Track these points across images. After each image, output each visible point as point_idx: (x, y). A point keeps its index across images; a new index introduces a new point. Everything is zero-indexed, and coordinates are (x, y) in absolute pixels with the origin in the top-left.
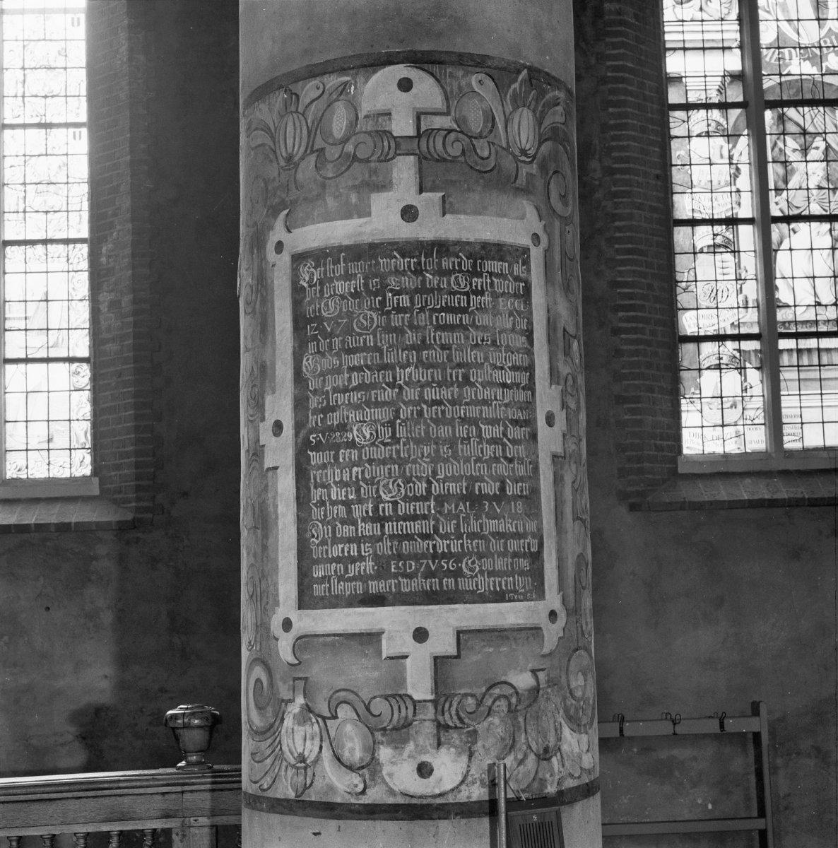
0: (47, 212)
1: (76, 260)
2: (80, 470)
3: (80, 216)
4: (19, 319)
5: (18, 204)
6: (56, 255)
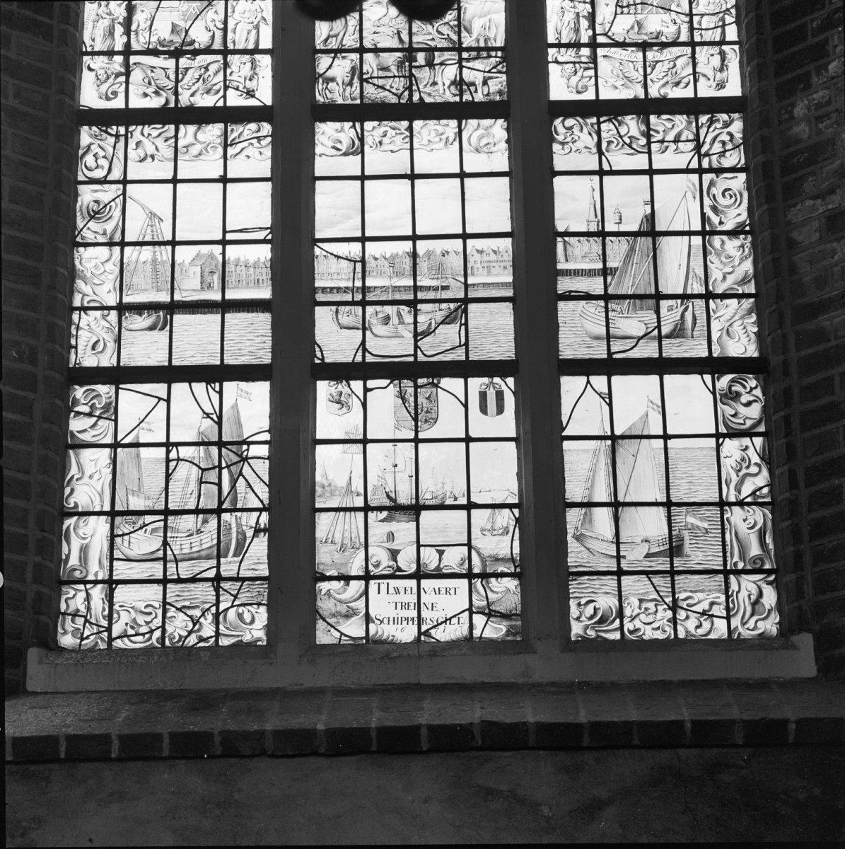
0: (644, 46)
1: (717, 148)
2: (751, 624)
4: (590, 273)
6: (671, 137)
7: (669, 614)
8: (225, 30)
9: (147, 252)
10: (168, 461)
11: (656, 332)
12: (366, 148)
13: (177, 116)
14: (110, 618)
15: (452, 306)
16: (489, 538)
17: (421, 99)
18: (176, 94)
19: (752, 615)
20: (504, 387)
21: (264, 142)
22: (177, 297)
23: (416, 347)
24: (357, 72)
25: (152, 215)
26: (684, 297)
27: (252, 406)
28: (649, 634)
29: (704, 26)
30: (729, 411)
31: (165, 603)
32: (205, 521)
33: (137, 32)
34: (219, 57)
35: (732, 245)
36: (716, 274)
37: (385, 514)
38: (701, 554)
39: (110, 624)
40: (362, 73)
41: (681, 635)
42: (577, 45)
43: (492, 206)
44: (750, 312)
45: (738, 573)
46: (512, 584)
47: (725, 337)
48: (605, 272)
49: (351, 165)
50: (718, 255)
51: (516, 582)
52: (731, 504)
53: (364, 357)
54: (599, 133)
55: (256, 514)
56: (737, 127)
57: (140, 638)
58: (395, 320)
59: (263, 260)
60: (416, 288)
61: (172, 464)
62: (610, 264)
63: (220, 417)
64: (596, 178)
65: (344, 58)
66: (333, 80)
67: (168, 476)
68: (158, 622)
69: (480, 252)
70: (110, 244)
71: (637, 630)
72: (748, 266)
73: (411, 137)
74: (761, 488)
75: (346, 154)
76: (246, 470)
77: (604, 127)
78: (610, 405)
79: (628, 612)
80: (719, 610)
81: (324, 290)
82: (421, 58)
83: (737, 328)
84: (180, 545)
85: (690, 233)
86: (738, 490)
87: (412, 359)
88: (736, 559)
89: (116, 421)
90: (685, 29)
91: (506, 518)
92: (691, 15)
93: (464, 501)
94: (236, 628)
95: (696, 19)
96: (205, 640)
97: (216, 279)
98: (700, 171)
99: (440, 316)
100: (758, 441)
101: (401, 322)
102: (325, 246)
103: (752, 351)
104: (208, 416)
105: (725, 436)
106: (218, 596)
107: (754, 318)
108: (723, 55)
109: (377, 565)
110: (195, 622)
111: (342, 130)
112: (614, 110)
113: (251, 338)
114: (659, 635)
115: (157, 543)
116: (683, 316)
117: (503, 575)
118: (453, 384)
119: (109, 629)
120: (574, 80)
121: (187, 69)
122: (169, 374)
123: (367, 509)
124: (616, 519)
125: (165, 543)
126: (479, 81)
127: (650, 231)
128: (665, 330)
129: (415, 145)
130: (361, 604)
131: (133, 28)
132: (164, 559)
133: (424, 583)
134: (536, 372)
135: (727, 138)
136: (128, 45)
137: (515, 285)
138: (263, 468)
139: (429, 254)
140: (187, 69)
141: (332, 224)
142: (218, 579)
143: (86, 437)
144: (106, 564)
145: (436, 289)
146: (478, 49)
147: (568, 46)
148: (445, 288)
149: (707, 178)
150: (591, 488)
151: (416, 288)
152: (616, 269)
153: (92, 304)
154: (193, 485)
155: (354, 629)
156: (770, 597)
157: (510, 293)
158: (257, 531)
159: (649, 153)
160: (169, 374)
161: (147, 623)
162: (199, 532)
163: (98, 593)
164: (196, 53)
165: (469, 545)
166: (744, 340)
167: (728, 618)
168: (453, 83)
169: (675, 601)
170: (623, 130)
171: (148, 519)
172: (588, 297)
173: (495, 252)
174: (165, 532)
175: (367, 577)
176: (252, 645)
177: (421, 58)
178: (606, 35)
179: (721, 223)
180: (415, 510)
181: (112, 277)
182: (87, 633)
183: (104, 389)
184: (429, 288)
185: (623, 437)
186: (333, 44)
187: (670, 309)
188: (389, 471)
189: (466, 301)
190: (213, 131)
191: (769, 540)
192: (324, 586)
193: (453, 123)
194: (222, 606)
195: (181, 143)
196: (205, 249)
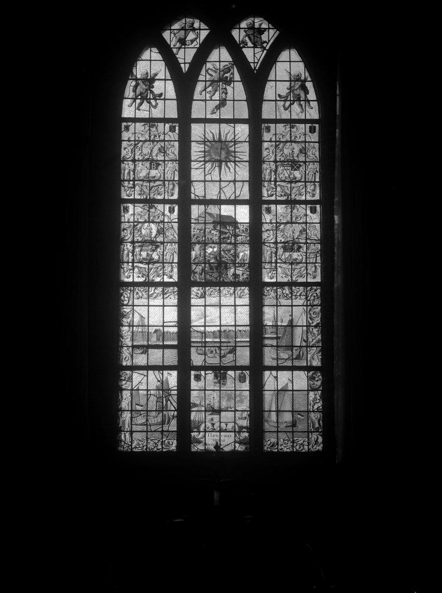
2: (315, 447)
3: (315, 266)
5: (271, 257)
7: (292, 444)
8: (163, 255)
9: (140, 329)
10: (148, 395)
11: (291, 358)
12: (206, 296)
13: (148, 284)
14: (131, 442)
15: (231, 348)
16: (241, 421)
17: (223, 280)
18: (148, 276)
19: (315, 445)
20: (246, 374)
21: (175, 294)
22: (150, 343)
23: (220, 361)
24: (203, 270)
25: (142, 317)
26: (301, 347)
27: (172, 378)
28: (285, 450)
29: (311, 257)
30: (312, 383)
31: (147, 438)
32: (159, 414)
33: (136, 255)
34: (162, 264)
35: (315, 331)
36: (310, 340)
37: (211, 412)
38: (301, 427)
39: (132, 444)
40: (205, 271)
41: (295, 451)
42: (271, 263)
43: (244, 316)
44: (319, 352)
45: (311, 432)
46: (247, 434)
47: (312, 360)
48: (277, 338)
49: (201, 301)
50: (311, 333)
51: (248, 434)
52: (311, 412)
53: (205, 363)
54: (277, 293)
55: (173, 412)
56: (319, 291)
57: (140, 448)
58: (214, 352)
59: (175, 332)
60: (221, 342)
61: (149, 396)
62: (279, 336)
63: (162, 381)
64: (276, 307)
65: (200, 265)
66: (196, 273)
67: (148, 399)
68: (145, 444)
69: (240, 331)
70: (129, 326)
71: (282, 449)
72: (320, 337)
73: (220, 292)
74: (319, 407)
75: (200, 298)
76: (170, 398)
77: (278, 290)
78: (277, 380)
79: (280, 443)
80: (306, 443)
81: (193, 342)
82: (223, 265)
83: (315, 357)
84: (152, 421)
85: (303, 326)
86: (313, 407)
87: (219, 365)
88: (311, 428)
89: (132, 382)
90: (304, 257)
91: (245, 414)
92: (306, 253)
93: (233, 409)
94: (168, 446)
95: (308, 254)
96: (159, 449)
97: (161, 338)
98: (307, 306)
99: (228, 351)
100: (320, 392)
101: (216, 353)
102: (195, 328)
103: (319, 364)
104: (159, 381)
105: (310, 391)
106: (162, 436)
107: (320, 354)
108: (315, 266)
109: (208, 428)
110: (156, 444)
111: (199, 290)
112: (281, 285)
113: (171, 357)
114: (288, 450)
115: (144, 420)
116: (300, 353)
117: (244, 432)
118: (231, 373)
119: (131, 445)
120: (270, 274)
121: (151, 268)
122: (148, 368)
123: (205, 411)
124: (277, 416)
125: (147, 420)
126: (241, 274)
127: (291, 325)
128: (294, 357)
129: (221, 295)
130: (203, 440)
131: (135, 254)
132: (147, 425)
133: (222, 433)
134: (256, 369)
135: (315, 295)
136: (133, 260)
137: (250, 342)
138: (175, 398)
139: (224, 331)
140: (151, 268)
141: (195, 321)
142: (162, 431)
143: (124, 387)
144: (130, 426)
145: (226, 342)
146: (241, 264)
147: (268, 263)
148: (230, 342)
149: (309, 308)
150: (271, 406)
151: (221, 342)
152: (280, 337)
153: (124, 345)
154: (155, 403)
155: (201, 447)
156: (320, 440)
157: (248, 344)
158: (174, 417)
159: (292, 299)
160: (148, 368)
161: (142, 444)
162: (157, 417)
163: (128, 435)
164: (155, 263)
165: (235, 423)
166: (317, 361)
167: (308, 446)
168: (233, 274)
169: (293, 440)
170: (284, 292)
171: (142, 412)
172: (272, 346)
173: (245, 331)
174: (147, 417)
175: (205, 431)
176: (172, 452)
177: (223, 265)
178: (280, 259)
179: (312, 323)
180: (219, 412)
181: (130, 337)
182: (125, 447)
183: (128, 372)
184: (224, 342)
185: (280, 390)
186: (197, 261)
187: (296, 350)
188: (213, 399)
189: (236, 346)
190: (160, 289)
191: (321, 422)
192: (193, 434)
193: (233, 288)
194: (164, 440)
195: (150, 293)
196: (158, 328)
